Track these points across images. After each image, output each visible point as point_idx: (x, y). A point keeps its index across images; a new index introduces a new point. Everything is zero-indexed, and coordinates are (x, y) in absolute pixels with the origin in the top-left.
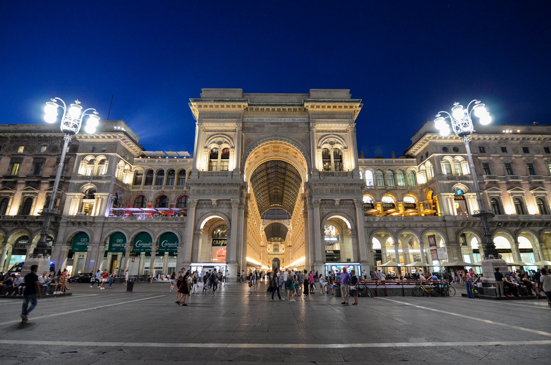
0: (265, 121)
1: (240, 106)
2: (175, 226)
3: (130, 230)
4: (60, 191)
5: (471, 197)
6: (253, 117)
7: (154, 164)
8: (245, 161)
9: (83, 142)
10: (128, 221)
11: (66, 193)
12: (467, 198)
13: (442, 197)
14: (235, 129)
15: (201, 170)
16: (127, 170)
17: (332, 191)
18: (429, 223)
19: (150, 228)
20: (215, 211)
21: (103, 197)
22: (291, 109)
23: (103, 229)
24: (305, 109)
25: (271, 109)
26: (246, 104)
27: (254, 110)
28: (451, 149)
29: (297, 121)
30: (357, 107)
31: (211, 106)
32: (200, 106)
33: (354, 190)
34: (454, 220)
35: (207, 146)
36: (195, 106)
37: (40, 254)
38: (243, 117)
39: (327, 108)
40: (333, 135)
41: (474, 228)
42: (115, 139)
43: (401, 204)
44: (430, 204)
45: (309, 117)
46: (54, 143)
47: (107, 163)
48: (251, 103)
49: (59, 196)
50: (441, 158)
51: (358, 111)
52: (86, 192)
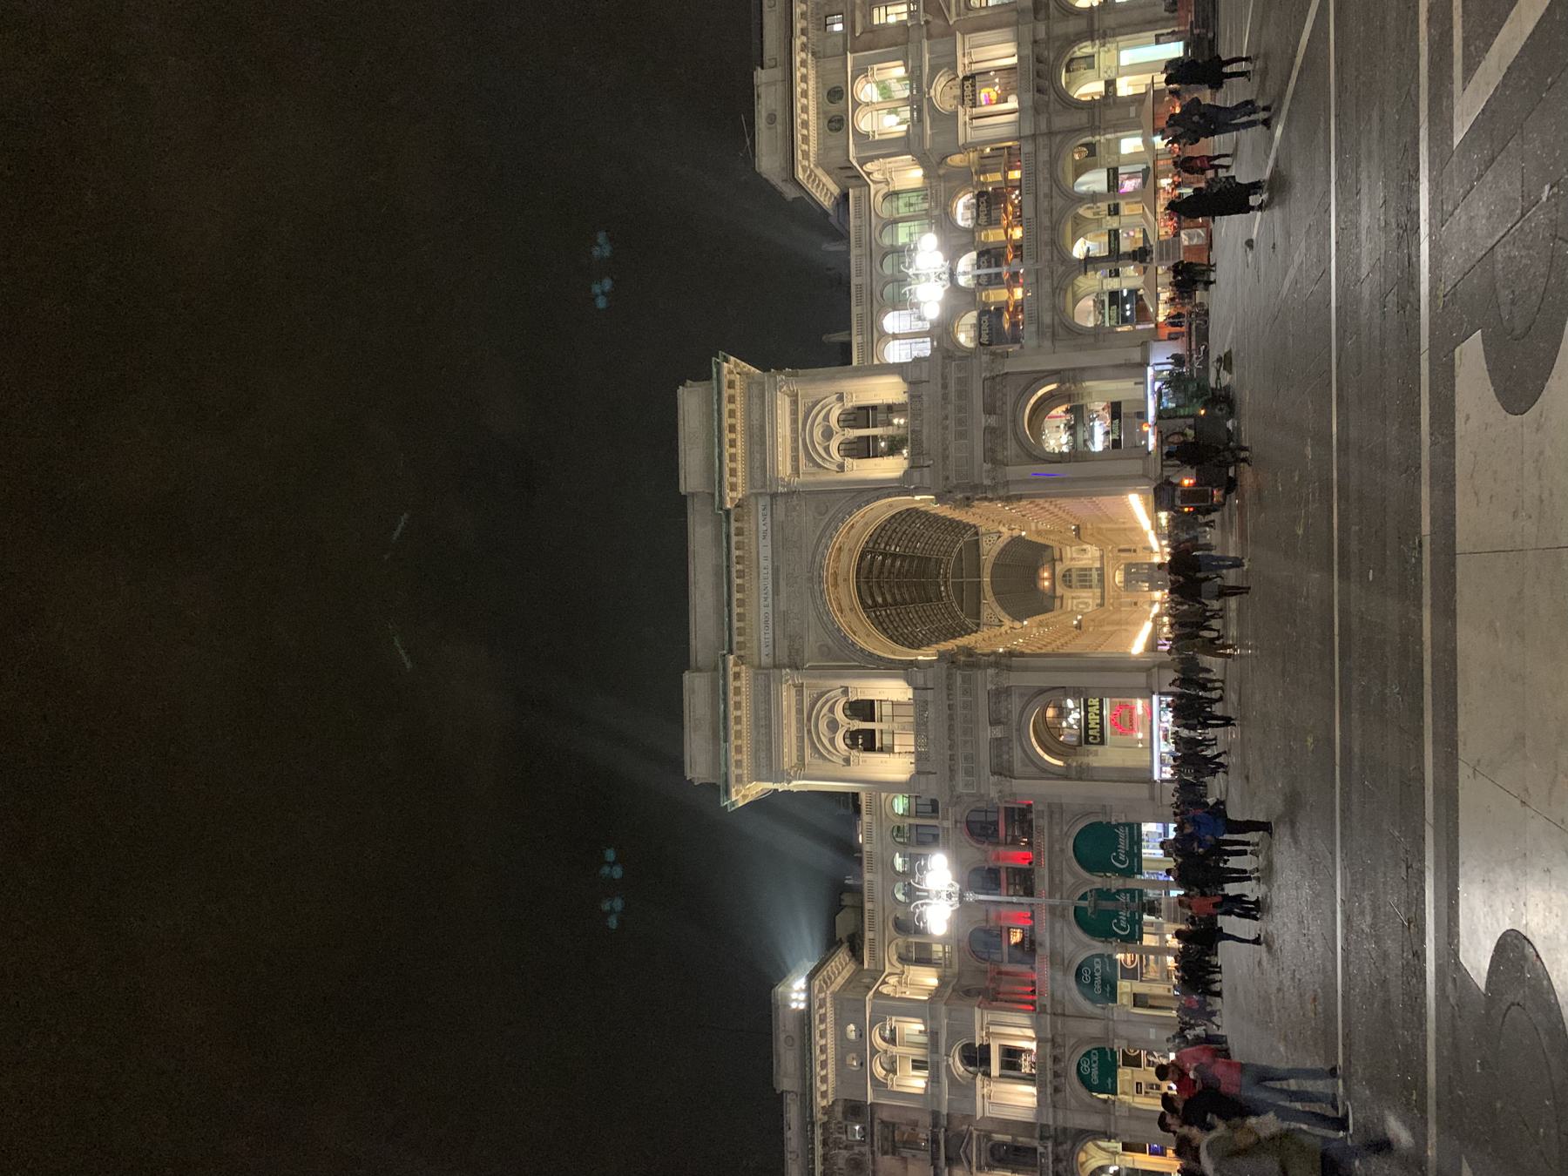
1: (737, 676)
2: (1057, 832)
4: (971, 1134)
8: (880, 658)
9: (836, 1090)
13: (969, 140)
17: (961, 435)
18: (1041, 177)
20: (1017, 730)
22: (736, 543)
23: (1069, 1016)
24: (737, 506)
25: (739, 596)
26: (731, 657)
27: (741, 639)
29: (769, 525)
30: (732, 368)
31: (739, 750)
32: (739, 779)
34: (1031, 112)
35: (844, 760)
36: (737, 792)
38: (760, 667)
39: (737, 449)
40: (804, 429)
41: (1052, 58)
42: (828, 1005)
43: (980, 236)
44: (982, 158)
45: (757, 495)
46: (840, 1169)
48: (726, 647)
50: (862, 138)
51: (736, 365)
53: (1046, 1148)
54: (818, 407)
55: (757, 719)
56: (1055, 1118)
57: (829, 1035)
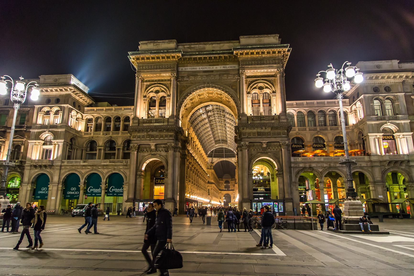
0: (198, 70)
3: (83, 171)
4: (23, 139)
5: (401, 136)
6: (187, 66)
7: (102, 112)
8: (180, 107)
10: (81, 164)
11: (28, 141)
12: (397, 138)
13: (370, 137)
14: (171, 79)
15: (140, 118)
16: (79, 118)
17: (259, 134)
19: (100, 170)
21: (59, 143)
22: (222, 57)
26: (180, 55)
28: (382, 89)
29: (228, 69)
32: (138, 59)
33: (280, 133)
36: (134, 59)
37: (2, 196)
39: (255, 53)
40: (262, 80)
41: (402, 167)
42: (66, 92)
47: (61, 113)
49: (23, 143)
52: (45, 139)
53: (17, 163)
54: (271, 85)
55: (165, 72)
56: (27, 166)
57: (56, 92)
